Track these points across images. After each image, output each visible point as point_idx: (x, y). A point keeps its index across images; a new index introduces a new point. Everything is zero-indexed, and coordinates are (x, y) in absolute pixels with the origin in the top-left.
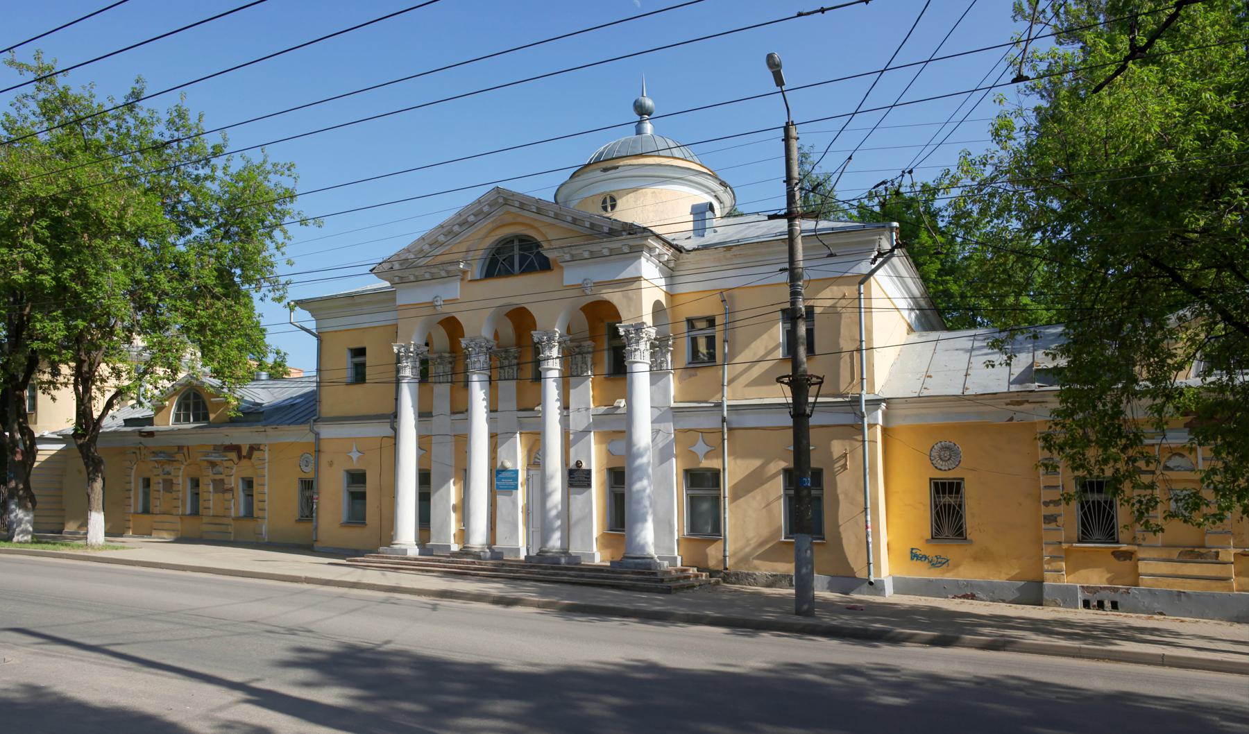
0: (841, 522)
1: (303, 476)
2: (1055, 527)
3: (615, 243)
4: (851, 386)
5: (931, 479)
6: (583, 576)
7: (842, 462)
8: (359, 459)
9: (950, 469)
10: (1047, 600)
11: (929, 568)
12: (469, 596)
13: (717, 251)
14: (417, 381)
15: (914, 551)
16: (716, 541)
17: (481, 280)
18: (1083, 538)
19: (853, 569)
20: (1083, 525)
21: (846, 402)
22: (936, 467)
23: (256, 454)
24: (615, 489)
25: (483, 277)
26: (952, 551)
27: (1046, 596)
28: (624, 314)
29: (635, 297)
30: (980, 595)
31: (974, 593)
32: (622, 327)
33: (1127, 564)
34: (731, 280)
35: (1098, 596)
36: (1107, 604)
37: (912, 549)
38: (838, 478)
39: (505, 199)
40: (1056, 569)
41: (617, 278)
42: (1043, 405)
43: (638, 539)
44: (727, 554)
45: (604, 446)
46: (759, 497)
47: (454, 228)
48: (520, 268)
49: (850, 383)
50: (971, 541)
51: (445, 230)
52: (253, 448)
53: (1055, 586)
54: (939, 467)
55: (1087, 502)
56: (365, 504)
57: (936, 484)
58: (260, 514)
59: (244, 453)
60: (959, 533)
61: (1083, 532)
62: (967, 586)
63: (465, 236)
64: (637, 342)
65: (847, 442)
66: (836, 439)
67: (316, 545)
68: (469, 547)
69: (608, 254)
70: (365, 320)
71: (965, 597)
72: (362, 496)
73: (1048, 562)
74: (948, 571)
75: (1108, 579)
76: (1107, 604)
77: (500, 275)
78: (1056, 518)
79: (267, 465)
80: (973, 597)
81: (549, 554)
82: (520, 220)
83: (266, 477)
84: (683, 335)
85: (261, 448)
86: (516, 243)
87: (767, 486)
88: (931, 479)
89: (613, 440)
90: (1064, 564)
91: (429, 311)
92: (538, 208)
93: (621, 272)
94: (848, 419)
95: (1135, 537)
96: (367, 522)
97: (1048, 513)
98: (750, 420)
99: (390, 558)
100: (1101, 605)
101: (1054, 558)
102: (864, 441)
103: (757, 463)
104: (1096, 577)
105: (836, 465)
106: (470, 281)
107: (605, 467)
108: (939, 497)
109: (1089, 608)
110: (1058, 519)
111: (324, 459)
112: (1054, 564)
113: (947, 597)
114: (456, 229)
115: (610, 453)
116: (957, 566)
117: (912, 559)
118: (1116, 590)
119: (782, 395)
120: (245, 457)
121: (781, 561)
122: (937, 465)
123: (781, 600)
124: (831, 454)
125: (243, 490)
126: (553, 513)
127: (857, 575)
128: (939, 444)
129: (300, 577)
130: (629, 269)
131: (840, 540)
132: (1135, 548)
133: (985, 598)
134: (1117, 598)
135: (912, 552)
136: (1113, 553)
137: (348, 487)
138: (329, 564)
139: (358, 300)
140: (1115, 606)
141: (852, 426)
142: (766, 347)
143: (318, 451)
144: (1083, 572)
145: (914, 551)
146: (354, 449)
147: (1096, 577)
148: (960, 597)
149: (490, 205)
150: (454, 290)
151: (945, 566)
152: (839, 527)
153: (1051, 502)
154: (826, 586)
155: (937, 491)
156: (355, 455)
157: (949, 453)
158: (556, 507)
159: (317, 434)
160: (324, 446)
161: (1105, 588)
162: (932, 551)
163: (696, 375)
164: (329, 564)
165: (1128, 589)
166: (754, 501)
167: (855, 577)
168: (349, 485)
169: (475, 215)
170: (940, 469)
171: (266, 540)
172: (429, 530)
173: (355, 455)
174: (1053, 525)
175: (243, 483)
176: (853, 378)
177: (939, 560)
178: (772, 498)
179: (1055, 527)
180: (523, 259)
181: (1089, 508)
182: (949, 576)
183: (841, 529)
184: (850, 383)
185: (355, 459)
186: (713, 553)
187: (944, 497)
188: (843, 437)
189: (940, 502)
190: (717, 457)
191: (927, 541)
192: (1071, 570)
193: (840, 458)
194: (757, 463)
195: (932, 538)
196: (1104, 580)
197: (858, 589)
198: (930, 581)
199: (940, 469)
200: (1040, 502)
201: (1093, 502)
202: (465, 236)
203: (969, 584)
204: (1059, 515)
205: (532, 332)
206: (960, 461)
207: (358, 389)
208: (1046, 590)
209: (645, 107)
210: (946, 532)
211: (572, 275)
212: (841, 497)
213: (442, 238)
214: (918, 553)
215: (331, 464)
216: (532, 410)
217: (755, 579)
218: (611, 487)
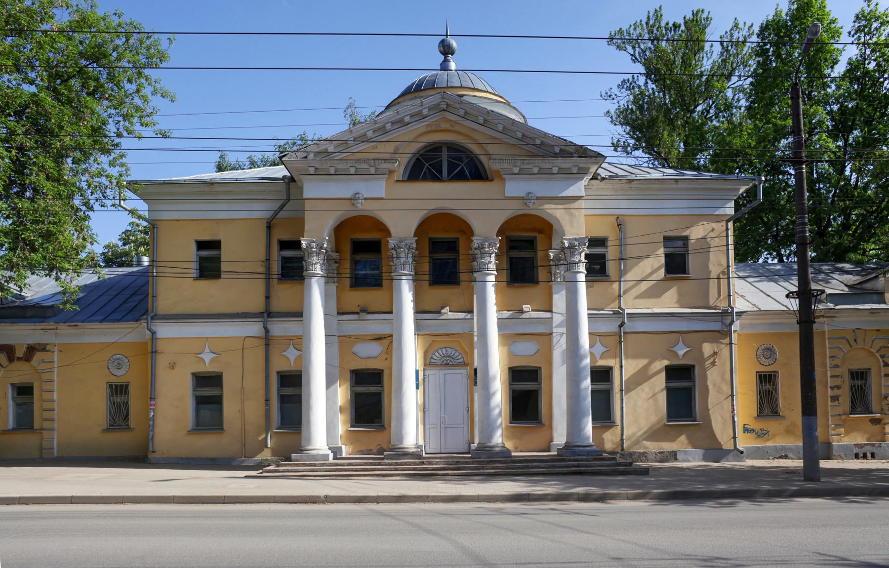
0: (710, 406)
1: (113, 380)
2: (838, 404)
3: (562, 163)
4: (719, 300)
5: (757, 372)
6: (528, 467)
7: (711, 360)
8: (213, 361)
9: (769, 365)
10: (835, 455)
11: (756, 439)
12: (550, 497)
13: (620, 182)
14: (410, 278)
15: (746, 426)
16: (612, 426)
17: (403, 181)
18: (852, 411)
19: (720, 443)
20: (852, 402)
21: (719, 313)
22: (760, 363)
23: (38, 356)
24: (514, 386)
25: (406, 179)
26: (772, 425)
27: (835, 453)
28: (567, 227)
29: (577, 214)
30: (790, 455)
31: (787, 454)
32: (304, 240)
33: (877, 427)
34: (624, 206)
35: (863, 450)
36: (869, 455)
37: (744, 425)
38: (709, 373)
39: (448, 105)
40: (838, 433)
41: (560, 195)
42: (835, 319)
43: (585, 431)
44: (624, 438)
45: (506, 348)
46: (647, 390)
47: (387, 125)
48: (448, 176)
49: (717, 299)
50: (783, 417)
51: (377, 125)
52: (32, 350)
53: (839, 445)
54: (763, 363)
55: (855, 386)
56: (221, 410)
57: (760, 376)
58: (46, 425)
59: (20, 353)
60: (775, 413)
61: (852, 407)
62: (782, 450)
63: (394, 135)
64: (398, 258)
65: (715, 345)
66: (706, 342)
67: (151, 456)
68: (404, 448)
69: (374, 173)
70: (221, 211)
71: (781, 457)
72: (217, 401)
73: (833, 429)
74: (768, 440)
75: (867, 439)
76: (869, 455)
77: (425, 179)
78: (838, 398)
79: (56, 369)
80: (786, 457)
81: (497, 449)
82: (457, 128)
83: (56, 382)
84: (716, 249)
85: (48, 348)
86: (445, 151)
87: (653, 380)
88: (757, 372)
89: (514, 342)
90: (843, 430)
91: (346, 206)
92: (485, 120)
93: (561, 193)
94: (717, 326)
95: (882, 409)
96: (224, 429)
97: (834, 394)
98: (640, 326)
99: (315, 465)
100: (865, 457)
101: (838, 426)
102: (731, 344)
103: (644, 362)
104: (859, 439)
105: (707, 363)
106: (397, 181)
107: (505, 367)
108: (762, 386)
109: (858, 459)
110: (840, 398)
111: (162, 362)
112: (837, 430)
113: (769, 459)
114: (389, 126)
115: (511, 355)
116: (774, 436)
117: (744, 432)
118: (873, 445)
119: (794, 304)
120: (19, 359)
121: (666, 441)
122: (761, 362)
123: (790, 472)
124: (702, 354)
125: (13, 399)
126: (497, 411)
127: (724, 447)
128: (763, 346)
129: (319, 497)
130: (571, 188)
131: (710, 421)
132: (884, 416)
133: (794, 457)
134: (874, 450)
135: (744, 427)
136: (870, 420)
137: (194, 390)
138: (246, 477)
139: (217, 188)
140: (873, 456)
141: (718, 331)
142: (652, 267)
143: (154, 352)
144: (853, 435)
145: (746, 426)
146: (207, 350)
147: (859, 439)
148: (777, 458)
149: (430, 109)
150: (377, 188)
151: (767, 436)
152: (709, 410)
153: (835, 386)
154: (702, 458)
155: (853, 378)
156: (207, 357)
157: (769, 352)
158: (498, 406)
159: (153, 333)
160: (160, 346)
161: (867, 444)
162: (757, 426)
163: (593, 287)
164: (246, 477)
165: (880, 444)
166: (643, 392)
167: (722, 449)
168: (194, 390)
169: (412, 116)
170: (763, 365)
171: (56, 455)
172: (301, 433)
173: (207, 357)
174: (836, 403)
175: (13, 390)
176: (719, 295)
177: (763, 432)
178: (657, 390)
179: (838, 404)
180: (451, 167)
181: (855, 390)
182: (769, 444)
183: (711, 412)
184: (717, 299)
185: (207, 361)
186: (610, 438)
187: (765, 386)
188: (712, 341)
189: (762, 389)
190: (615, 357)
191: (755, 418)
192: (847, 433)
193: (710, 357)
194: (644, 362)
195: (758, 416)
196: (865, 439)
197: (725, 458)
198: (757, 447)
199: (763, 365)
200: (827, 387)
201: (858, 386)
202: (394, 135)
203: (783, 448)
204: (840, 396)
205: (388, 239)
206: (776, 359)
207: (206, 285)
208: (835, 448)
209: (452, 48)
210: (766, 411)
211: (515, 188)
212: (710, 386)
213: (370, 134)
214: (749, 427)
215: (172, 366)
216: (439, 312)
217: (646, 457)
218: (510, 384)
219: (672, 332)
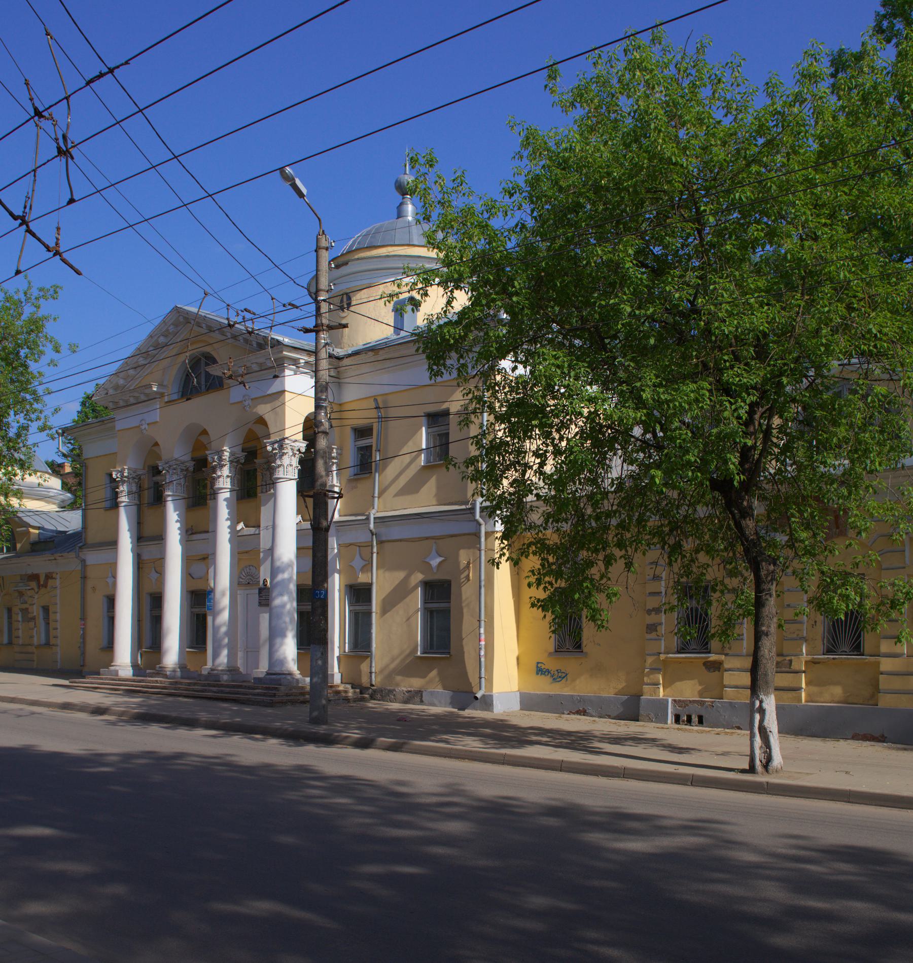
2: (657, 637)
7: (465, 574)
15: (539, 665)
23: (50, 582)
26: (570, 664)
27: (642, 712)
28: (272, 429)
30: (590, 710)
36: (695, 719)
37: (538, 663)
38: (463, 589)
43: (278, 654)
44: (373, 670)
50: (586, 653)
52: (49, 576)
71: (578, 712)
76: (695, 719)
80: (583, 712)
98: (396, 532)
101: (655, 670)
103: (400, 575)
104: (689, 690)
110: (658, 628)
117: (537, 674)
118: (702, 703)
120: (42, 586)
131: (463, 653)
132: (723, 657)
133: (594, 714)
135: (537, 667)
136: (705, 664)
145: (539, 665)
147: (689, 690)
153: (654, 609)
154: (449, 700)
159: (83, 561)
161: (694, 702)
162: (551, 665)
165: (712, 702)
166: (398, 613)
183: (464, 642)
191: (550, 654)
194: (400, 575)
195: (556, 651)
196: (696, 693)
201: (692, 609)
203: (582, 700)
208: (642, 704)
211: (236, 393)
217: (394, 695)
219: (400, 540)
